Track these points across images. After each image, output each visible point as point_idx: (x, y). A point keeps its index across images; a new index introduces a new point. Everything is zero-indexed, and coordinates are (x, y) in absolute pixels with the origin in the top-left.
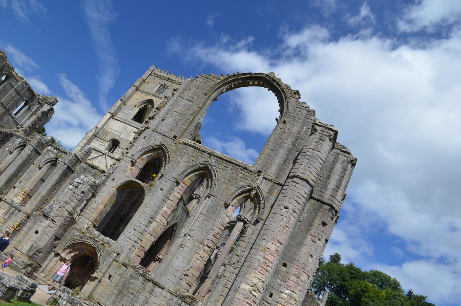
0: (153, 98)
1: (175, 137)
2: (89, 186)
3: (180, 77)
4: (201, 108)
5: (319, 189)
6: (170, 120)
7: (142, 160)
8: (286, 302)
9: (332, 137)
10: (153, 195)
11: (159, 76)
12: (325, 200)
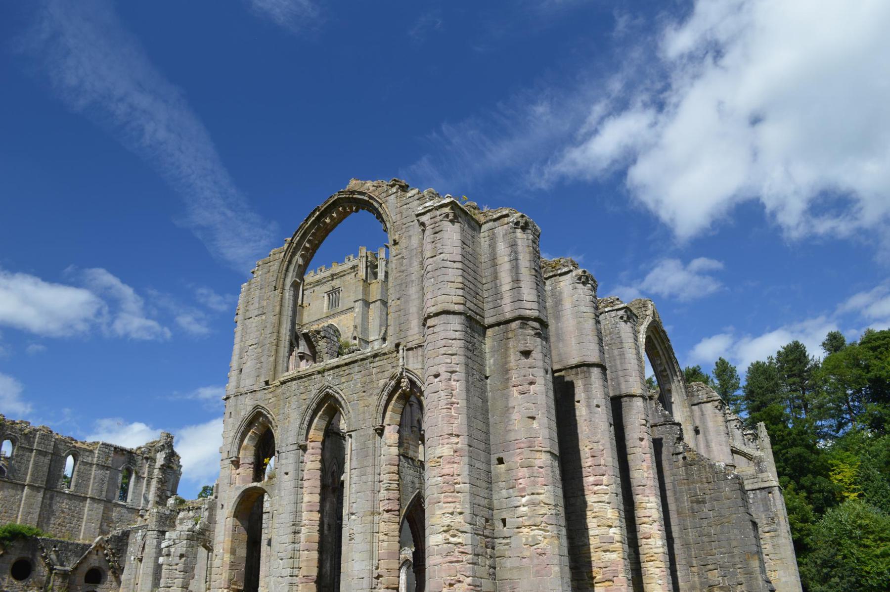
0: (330, 322)
1: (267, 383)
2: (185, 542)
3: (346, 260)
4: (280, 313)
5: (491, 305)
6: (249, 364)
7: (245, 449)
8: (530, 518)
9: (451, 217)
10: (279, 490)
11: (317, 282)
12: (508, 316)
